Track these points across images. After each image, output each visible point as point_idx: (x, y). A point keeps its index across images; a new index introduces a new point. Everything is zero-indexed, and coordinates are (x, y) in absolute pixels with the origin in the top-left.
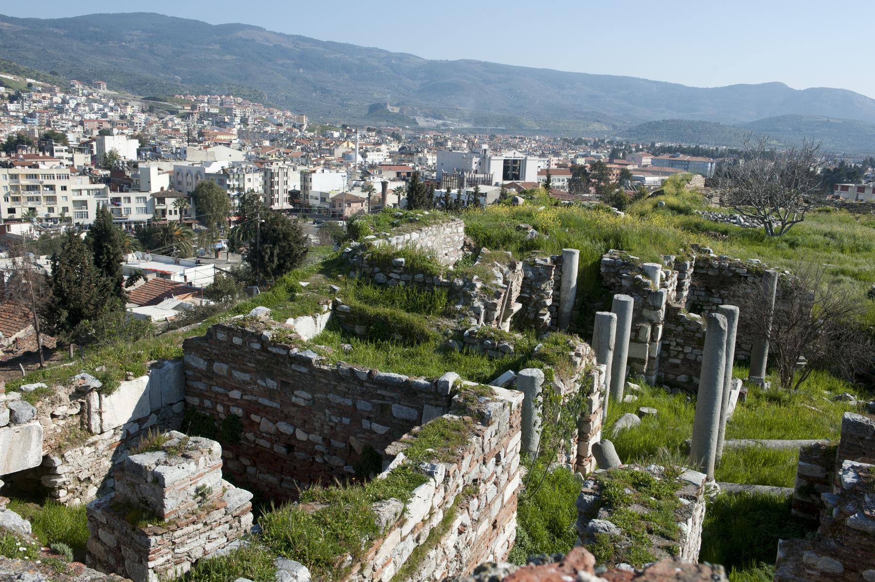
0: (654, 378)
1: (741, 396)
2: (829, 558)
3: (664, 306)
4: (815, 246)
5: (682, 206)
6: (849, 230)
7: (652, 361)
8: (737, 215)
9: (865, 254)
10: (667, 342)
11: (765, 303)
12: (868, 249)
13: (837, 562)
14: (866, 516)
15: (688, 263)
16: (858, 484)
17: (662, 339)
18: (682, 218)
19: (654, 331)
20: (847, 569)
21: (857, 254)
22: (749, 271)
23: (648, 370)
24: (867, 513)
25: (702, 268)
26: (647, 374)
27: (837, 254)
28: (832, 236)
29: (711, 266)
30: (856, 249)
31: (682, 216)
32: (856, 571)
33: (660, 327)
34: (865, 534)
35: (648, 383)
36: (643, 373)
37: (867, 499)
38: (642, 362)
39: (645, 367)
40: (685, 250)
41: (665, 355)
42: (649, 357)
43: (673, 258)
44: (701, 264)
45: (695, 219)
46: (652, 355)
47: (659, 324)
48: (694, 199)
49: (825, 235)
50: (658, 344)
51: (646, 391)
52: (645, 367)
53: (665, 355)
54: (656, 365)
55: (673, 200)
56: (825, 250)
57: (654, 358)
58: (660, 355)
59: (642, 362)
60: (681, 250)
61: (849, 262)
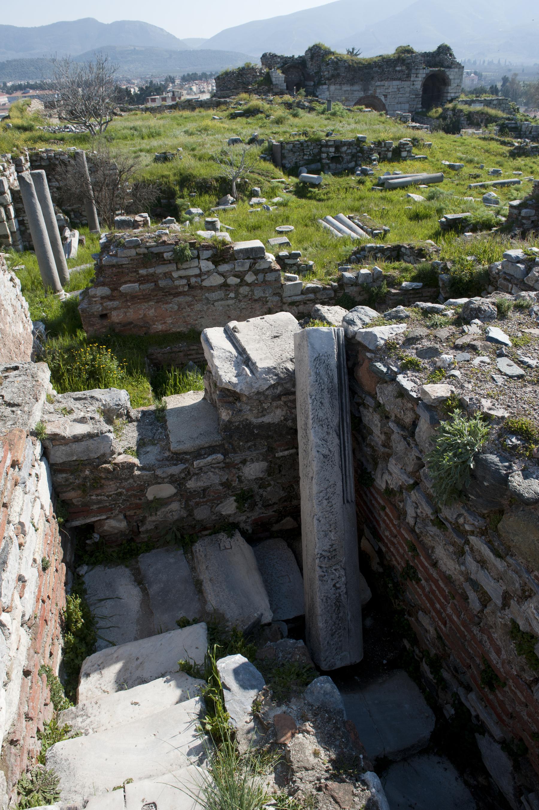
0: (20, 247)
1: (81, 242)
2: (101, 288)
3: (8, 192)
4: (125, 138)
5: (25, 124)
6: (147, 123)
7: (14, 235)
8: (70, 126)
9: (157, 138)
10: (21, 218)
11: (83, 175)
12: (159, 134)
13: (106, 288)
14: (111, 255)
15: (22, 158)
16: (107, 242)
17: (16, 217)
18: (28, 134)
19: (7, 212)
20: (113, 290)
21: (152, 139)
22: (70, 157)
23: (14, 242)
24: (111, 253)
25: (36, 161)
26: (14, 245)
27: (139, 140)
28: (135, 128)
29: (42, 158)
30: (151, 135)
31: (27, 133)
32: (117, 290)
33: (11, 208)
34: (113, 266)
35: (17, 251)
36: (10, 245)
37: (112, 247)
38: (7, 237)
39: (10, 239)
40: (17, 148)
41: (23, 228)
42: (11, 232)
43: (9, 156)
44: (34, 158)
45: (38, 134)
46: (12, 230)
47: (9, 205)
48: (36, 119)
49: (131, 129)
50: (14, 222)
51: (15, 256)
52: (10, 239)
53: (23, 228)
54: (18, 237)
55: (18, 122)
56: (131, 140)
57: (14, 232)
58: (19, 229)
59: (7, 237)
60: (15, 149)
61: (145, 144)
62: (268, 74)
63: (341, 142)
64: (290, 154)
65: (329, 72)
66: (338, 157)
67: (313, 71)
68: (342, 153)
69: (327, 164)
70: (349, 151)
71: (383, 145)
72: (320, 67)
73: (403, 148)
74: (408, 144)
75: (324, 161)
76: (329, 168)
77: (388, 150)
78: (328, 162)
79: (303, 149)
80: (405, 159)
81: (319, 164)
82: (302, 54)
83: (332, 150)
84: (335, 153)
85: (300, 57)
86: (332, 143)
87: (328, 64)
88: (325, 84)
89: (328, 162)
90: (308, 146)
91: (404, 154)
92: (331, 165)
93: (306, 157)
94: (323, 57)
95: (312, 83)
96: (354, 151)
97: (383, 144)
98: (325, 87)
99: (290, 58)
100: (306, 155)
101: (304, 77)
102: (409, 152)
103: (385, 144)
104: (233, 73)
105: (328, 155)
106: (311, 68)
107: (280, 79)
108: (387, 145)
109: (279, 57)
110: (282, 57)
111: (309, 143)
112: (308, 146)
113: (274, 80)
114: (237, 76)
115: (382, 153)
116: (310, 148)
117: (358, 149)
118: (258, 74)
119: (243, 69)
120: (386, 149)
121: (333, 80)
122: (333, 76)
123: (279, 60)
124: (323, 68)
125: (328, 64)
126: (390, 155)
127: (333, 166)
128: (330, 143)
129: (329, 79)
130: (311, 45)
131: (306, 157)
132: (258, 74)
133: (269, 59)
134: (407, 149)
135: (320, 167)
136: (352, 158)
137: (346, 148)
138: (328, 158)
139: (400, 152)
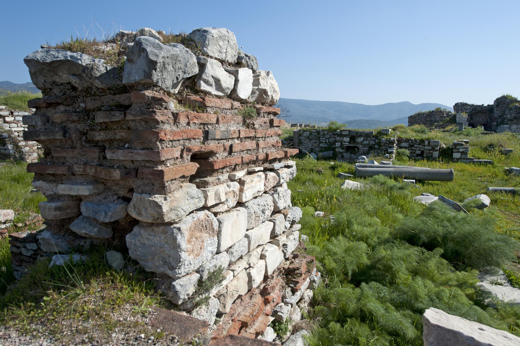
62: (455, 116)
63: (357, 132)
64: (307, 141)
65: (511, 115)
66: (355, 147)
67: (498, 114)
68: (357, 143)
69: (341, 153)
70: (366, 142)
71: (426, 143)
72: (504, 112)
73: (455, 149)
74: (462, 145)
75: (337, 150)
76: (343, 157)
77: (433, 149)
78: (341, 150)
79: (319, 137)
80: (458, 160)
81: (332, 152)
82: (491, 102)
83: (347, 139)
84: (349, 142)
85: (488, 105)
86: (347, 133)
87: (511, 109)
88: (507, 124)
89: (341, 150)
90: (324, 135)
91: (456, 155)
92: (344, 154)
93: (321, 145)
94: (508, 104)
95: (495, 123)
96: (372, 142)
97: (426, 143)
98: (505, 126)
99: (480, 106)
100: (322, 142)
101: (491, 120)
102: (464, 153)
103: (429, 143)
104: (424, 114)
105: (342, 144)
106: (497, 113)
107: (463, 119)
108: (431, 144)
109: (470, 105)
110: (472, 105)
111: (326, 132)
112: (324, 135)
113: (457, 119)
114: (427, 116)
115: (425, 151)
116: (326, 136)
117: (377, 141)
118: (445, 115)
119: (433, 111)
120: (430, 148)
121: (515, 121)
122: (515, 118)
123: (469, 107)
124: (507, 112)
125: (511, 109)
126: (436, 154)
127: (347, 155)
128: (344, 133)
129: (510, 120)
130: (499, 96)
131: (321, 145)
132: (445, 115)
133: (459, 107)
134: (461, 150)
135: (331, 155)
136: (369, 150)
137: (362, 139)
138: (342, 147)
139: (452, 152)
